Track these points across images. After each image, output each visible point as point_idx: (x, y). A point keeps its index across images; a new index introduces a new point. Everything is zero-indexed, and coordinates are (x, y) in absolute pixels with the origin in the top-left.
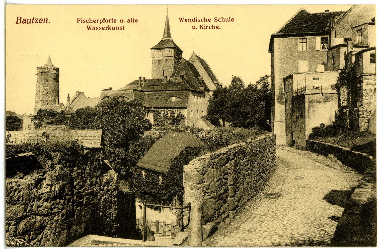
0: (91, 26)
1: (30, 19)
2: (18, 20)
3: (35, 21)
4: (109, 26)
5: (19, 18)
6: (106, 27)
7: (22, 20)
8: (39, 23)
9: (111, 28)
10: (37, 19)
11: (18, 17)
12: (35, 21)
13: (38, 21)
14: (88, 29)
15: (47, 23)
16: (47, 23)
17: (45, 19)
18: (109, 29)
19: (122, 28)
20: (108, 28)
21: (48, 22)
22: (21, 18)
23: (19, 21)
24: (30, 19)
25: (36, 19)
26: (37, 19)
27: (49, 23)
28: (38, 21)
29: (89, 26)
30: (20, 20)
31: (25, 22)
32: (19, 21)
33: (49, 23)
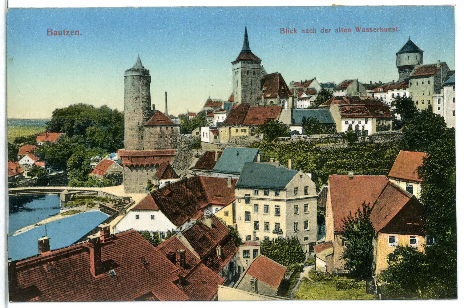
1: (61, 32)
6: (378, 29)
7: (53, 32)
10: (68, 32)
15: (78, 34)
16: (78, 34)
17: (76, 32)
20: (379, 30)
21: (79, 34)
22: (52, 30)
23: (50, 33)
25: (66, 31)
26: (68, 32)
27: (81, 34)
30: (50, 32)
31: (56, 34)
32: (50, 33)
33: (81, 34)
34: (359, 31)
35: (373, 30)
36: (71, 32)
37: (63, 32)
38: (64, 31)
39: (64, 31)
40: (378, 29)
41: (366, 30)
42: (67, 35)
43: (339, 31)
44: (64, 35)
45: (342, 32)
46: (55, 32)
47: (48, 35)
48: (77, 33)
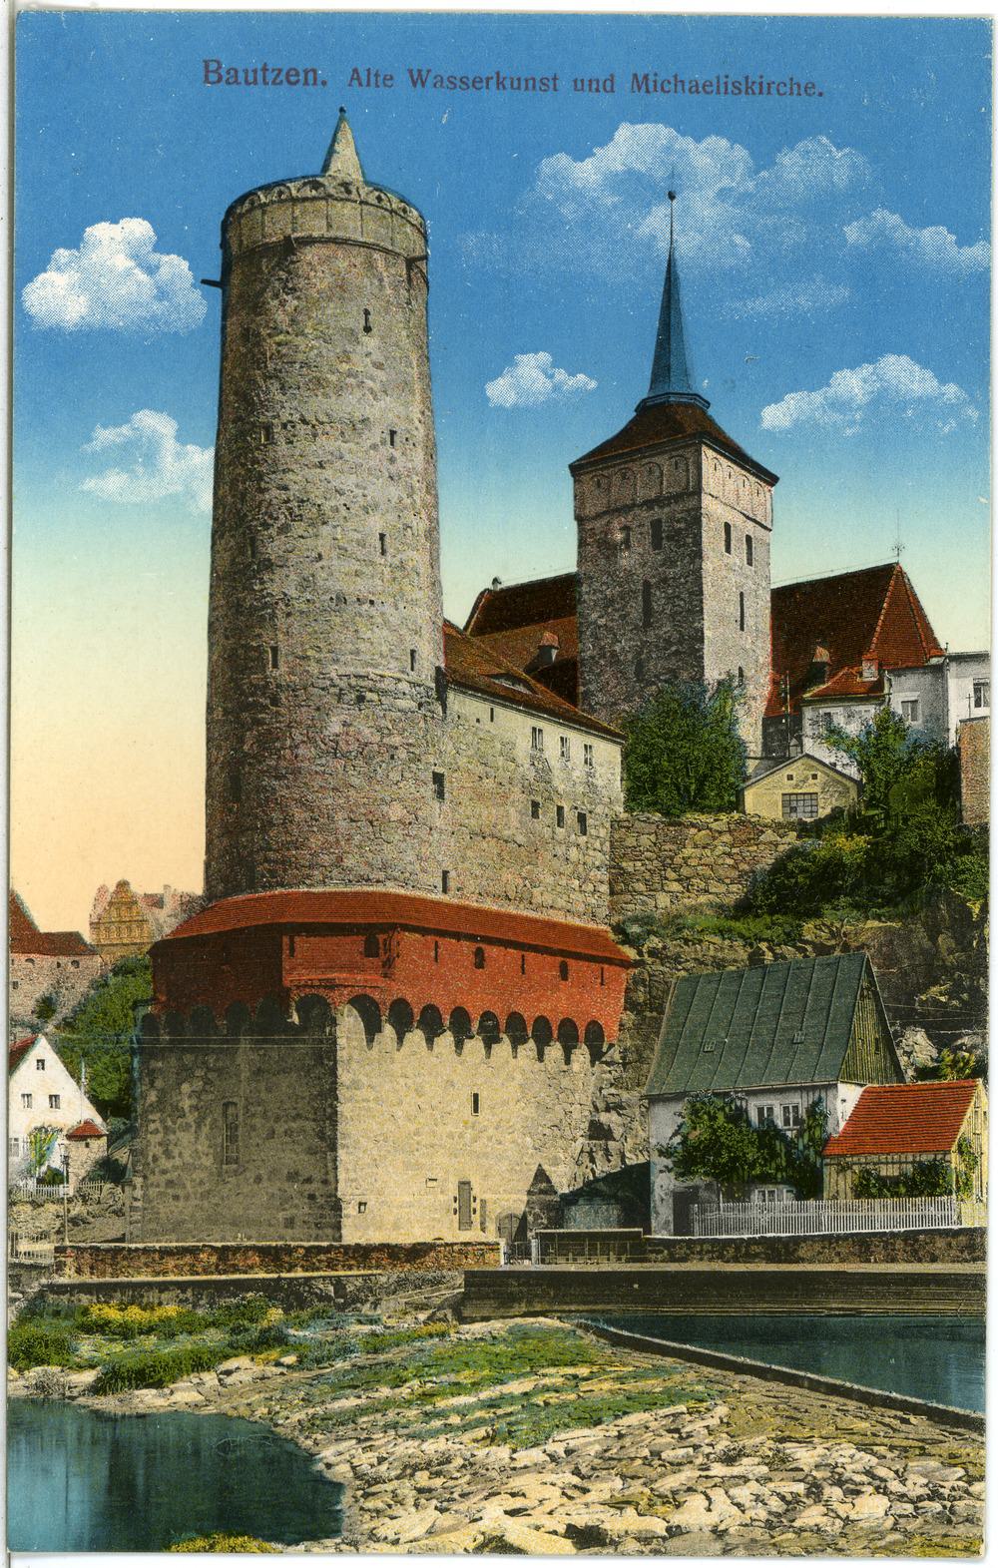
0: (429, 71)
2: (207, 71)
3: (270, 76)
4: (498, 74)
5: (213, 66)
6: (488, 79)
7: (223, 72)
8: (285, 82)
9: (507, 83)
10: (280, 71)
11: (207, 63)
12: (270, 76)
13: (283, 77)
14: (415, 84)
17: (306, 72)
18: (498, 88)
19: (551, 84)
20: (493, 83)
22: (220, 67)
23: (213, 77)
24: (255, 71)
25: (273, 70)
26: (280, 71)
27: (324, 83)
28: (283, 77)
29: (420, 71)
34: (423, 84)
35: (470, 83)
36: (288, 75)
37: (260, 74)
38: (265, 69)
39: (265, 69)
40: (488, 79)
41: (446, 83)
42: (274, 83)
43: (364, 82)
44: (265, 83)
45: (378, 86)
46: (228, 72)
47: (207, 80)
48: (311, 76)
